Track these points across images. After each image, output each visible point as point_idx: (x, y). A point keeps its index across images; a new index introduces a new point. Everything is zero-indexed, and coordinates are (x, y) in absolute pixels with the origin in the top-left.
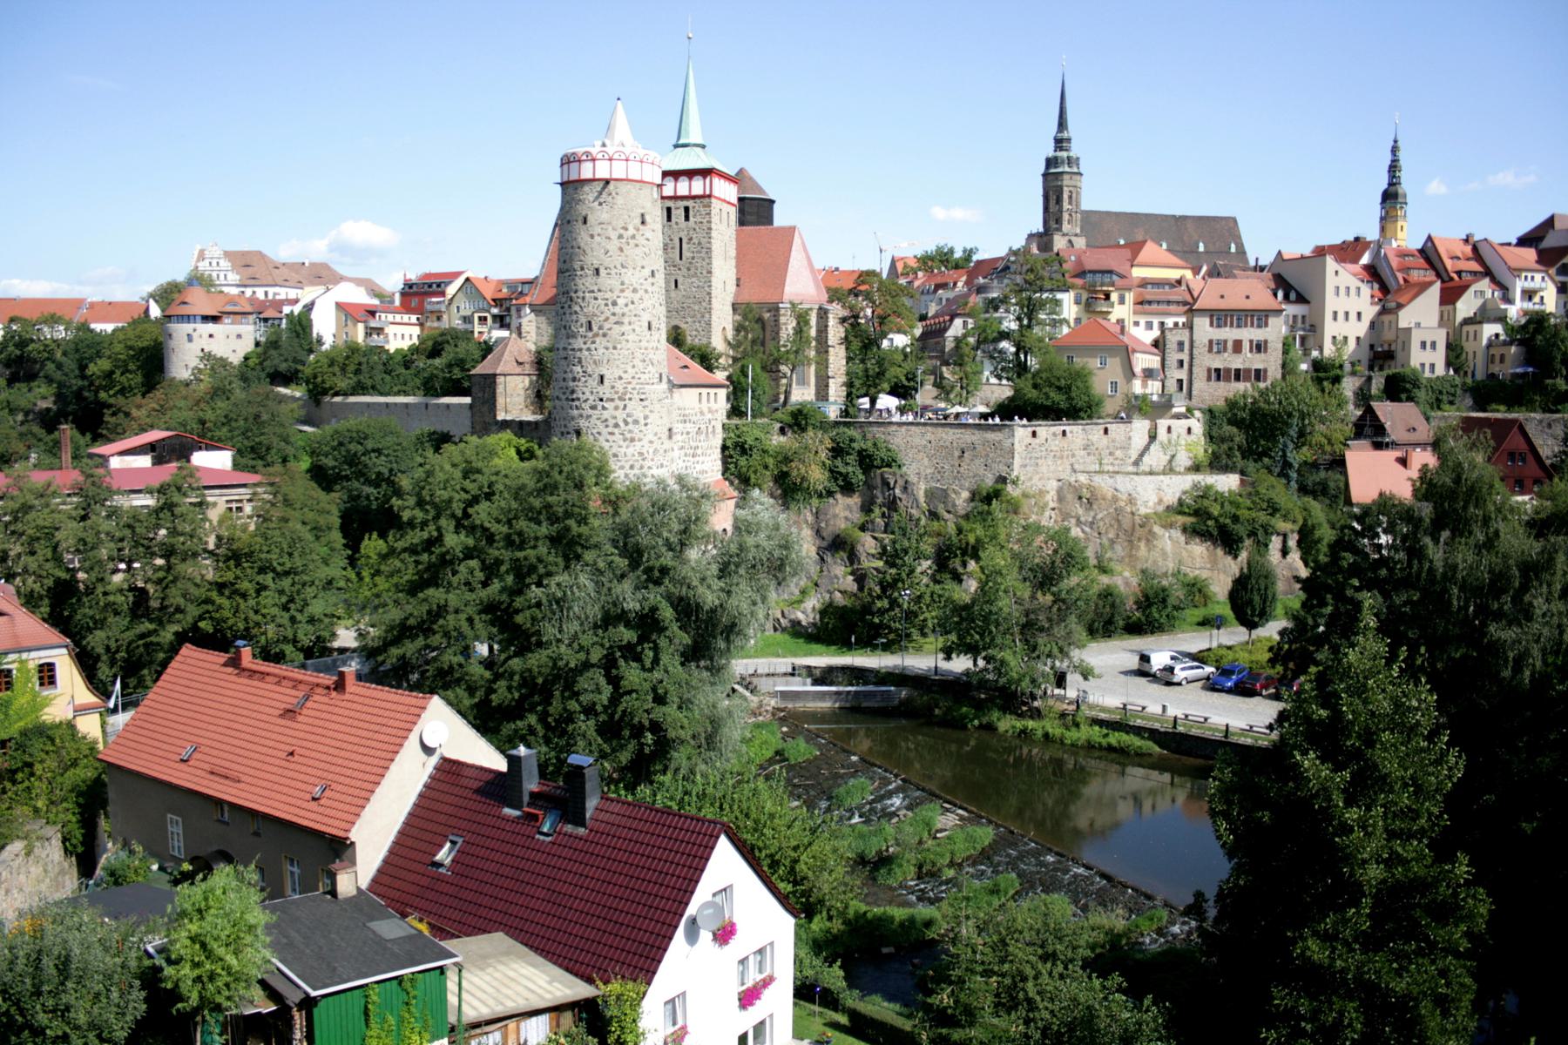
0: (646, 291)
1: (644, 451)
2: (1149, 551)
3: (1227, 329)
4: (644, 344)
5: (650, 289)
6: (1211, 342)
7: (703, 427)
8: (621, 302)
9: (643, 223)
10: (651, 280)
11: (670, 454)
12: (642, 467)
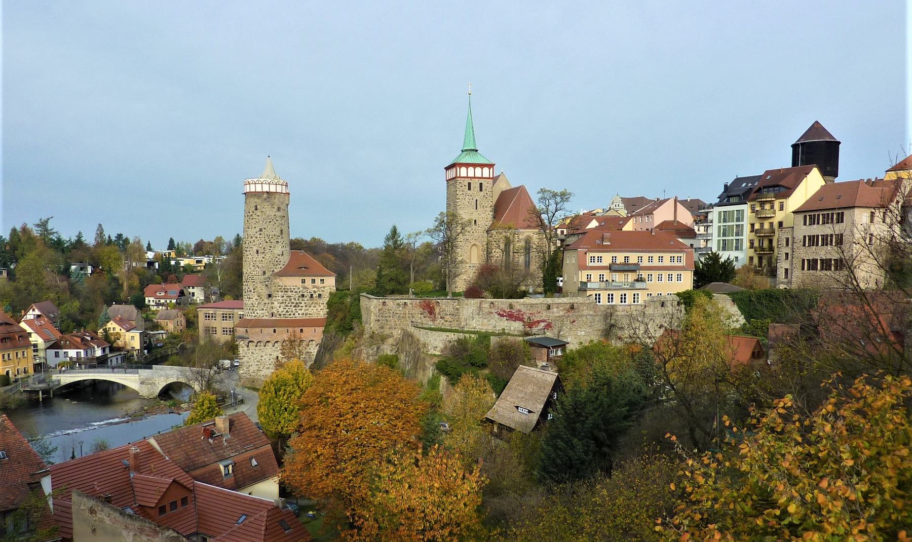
0: (256, 237)
1: (254, 303)
2: (424, 375)
3: (815, 226)
4: (254, 259)
5: (258, 236)
6: (805, 237)
7: (306, 294)
8: (247, 242)
9: (256, 209)
10: (259, 233)
11: (270, 305)
12: (253, 310)
